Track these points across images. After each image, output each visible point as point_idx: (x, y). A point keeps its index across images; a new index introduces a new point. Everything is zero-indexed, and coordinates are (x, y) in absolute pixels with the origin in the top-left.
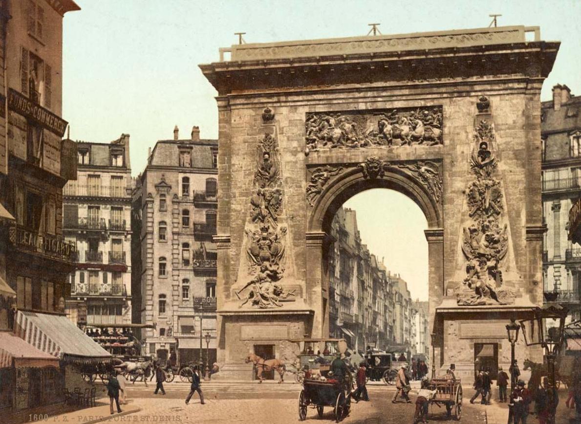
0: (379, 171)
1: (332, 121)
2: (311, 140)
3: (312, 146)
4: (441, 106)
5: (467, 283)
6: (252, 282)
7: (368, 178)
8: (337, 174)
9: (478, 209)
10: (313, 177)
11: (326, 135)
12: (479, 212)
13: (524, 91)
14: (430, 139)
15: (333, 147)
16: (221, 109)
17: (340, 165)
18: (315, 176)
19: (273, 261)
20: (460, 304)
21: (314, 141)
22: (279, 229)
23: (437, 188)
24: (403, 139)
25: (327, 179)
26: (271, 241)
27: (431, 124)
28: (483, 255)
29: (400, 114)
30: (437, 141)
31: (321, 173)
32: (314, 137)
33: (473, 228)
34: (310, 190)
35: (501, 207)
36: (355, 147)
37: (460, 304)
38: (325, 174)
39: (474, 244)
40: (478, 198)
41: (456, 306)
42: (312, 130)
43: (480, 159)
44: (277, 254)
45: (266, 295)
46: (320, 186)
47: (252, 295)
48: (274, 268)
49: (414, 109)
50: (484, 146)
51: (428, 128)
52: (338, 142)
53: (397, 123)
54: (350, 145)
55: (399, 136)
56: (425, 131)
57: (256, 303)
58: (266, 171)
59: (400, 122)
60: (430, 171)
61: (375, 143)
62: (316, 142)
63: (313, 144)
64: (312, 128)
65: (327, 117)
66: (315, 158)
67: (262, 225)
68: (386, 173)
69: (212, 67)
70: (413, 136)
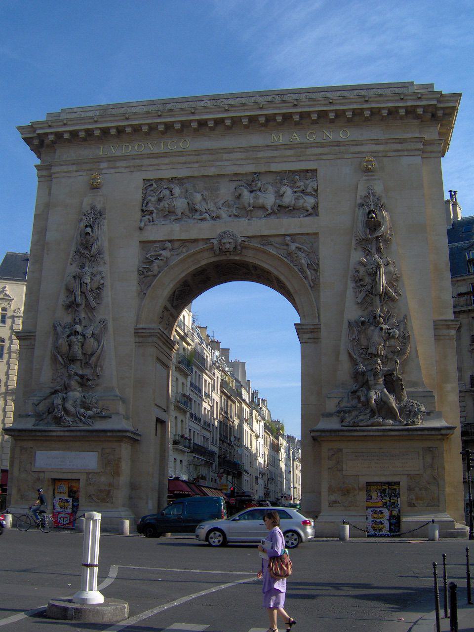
0: (235, 248)
4: (315, 171)
10: (148, 256)
13: (420, 153)
16: (43, 179)
17: (184, 242)
20: (343, 424)
21: (152, 213)
27: (303, 191)
31: (158, 253)
35: (397, 293)
36: (202, 220)
37: (343, 424)
38: (164, 253)
39: (364, 342)
40: (367, 280)
42: (150, 200)
46: (156, 268)
51: (299, 196)
53: (260, 190)
55: (263, 207)
56: (297, 199)
57: (58, 420)
61: (230, 216)
62: (154, 215)
64: (150, 198)
69: (32, 127)
70: (279, 206)
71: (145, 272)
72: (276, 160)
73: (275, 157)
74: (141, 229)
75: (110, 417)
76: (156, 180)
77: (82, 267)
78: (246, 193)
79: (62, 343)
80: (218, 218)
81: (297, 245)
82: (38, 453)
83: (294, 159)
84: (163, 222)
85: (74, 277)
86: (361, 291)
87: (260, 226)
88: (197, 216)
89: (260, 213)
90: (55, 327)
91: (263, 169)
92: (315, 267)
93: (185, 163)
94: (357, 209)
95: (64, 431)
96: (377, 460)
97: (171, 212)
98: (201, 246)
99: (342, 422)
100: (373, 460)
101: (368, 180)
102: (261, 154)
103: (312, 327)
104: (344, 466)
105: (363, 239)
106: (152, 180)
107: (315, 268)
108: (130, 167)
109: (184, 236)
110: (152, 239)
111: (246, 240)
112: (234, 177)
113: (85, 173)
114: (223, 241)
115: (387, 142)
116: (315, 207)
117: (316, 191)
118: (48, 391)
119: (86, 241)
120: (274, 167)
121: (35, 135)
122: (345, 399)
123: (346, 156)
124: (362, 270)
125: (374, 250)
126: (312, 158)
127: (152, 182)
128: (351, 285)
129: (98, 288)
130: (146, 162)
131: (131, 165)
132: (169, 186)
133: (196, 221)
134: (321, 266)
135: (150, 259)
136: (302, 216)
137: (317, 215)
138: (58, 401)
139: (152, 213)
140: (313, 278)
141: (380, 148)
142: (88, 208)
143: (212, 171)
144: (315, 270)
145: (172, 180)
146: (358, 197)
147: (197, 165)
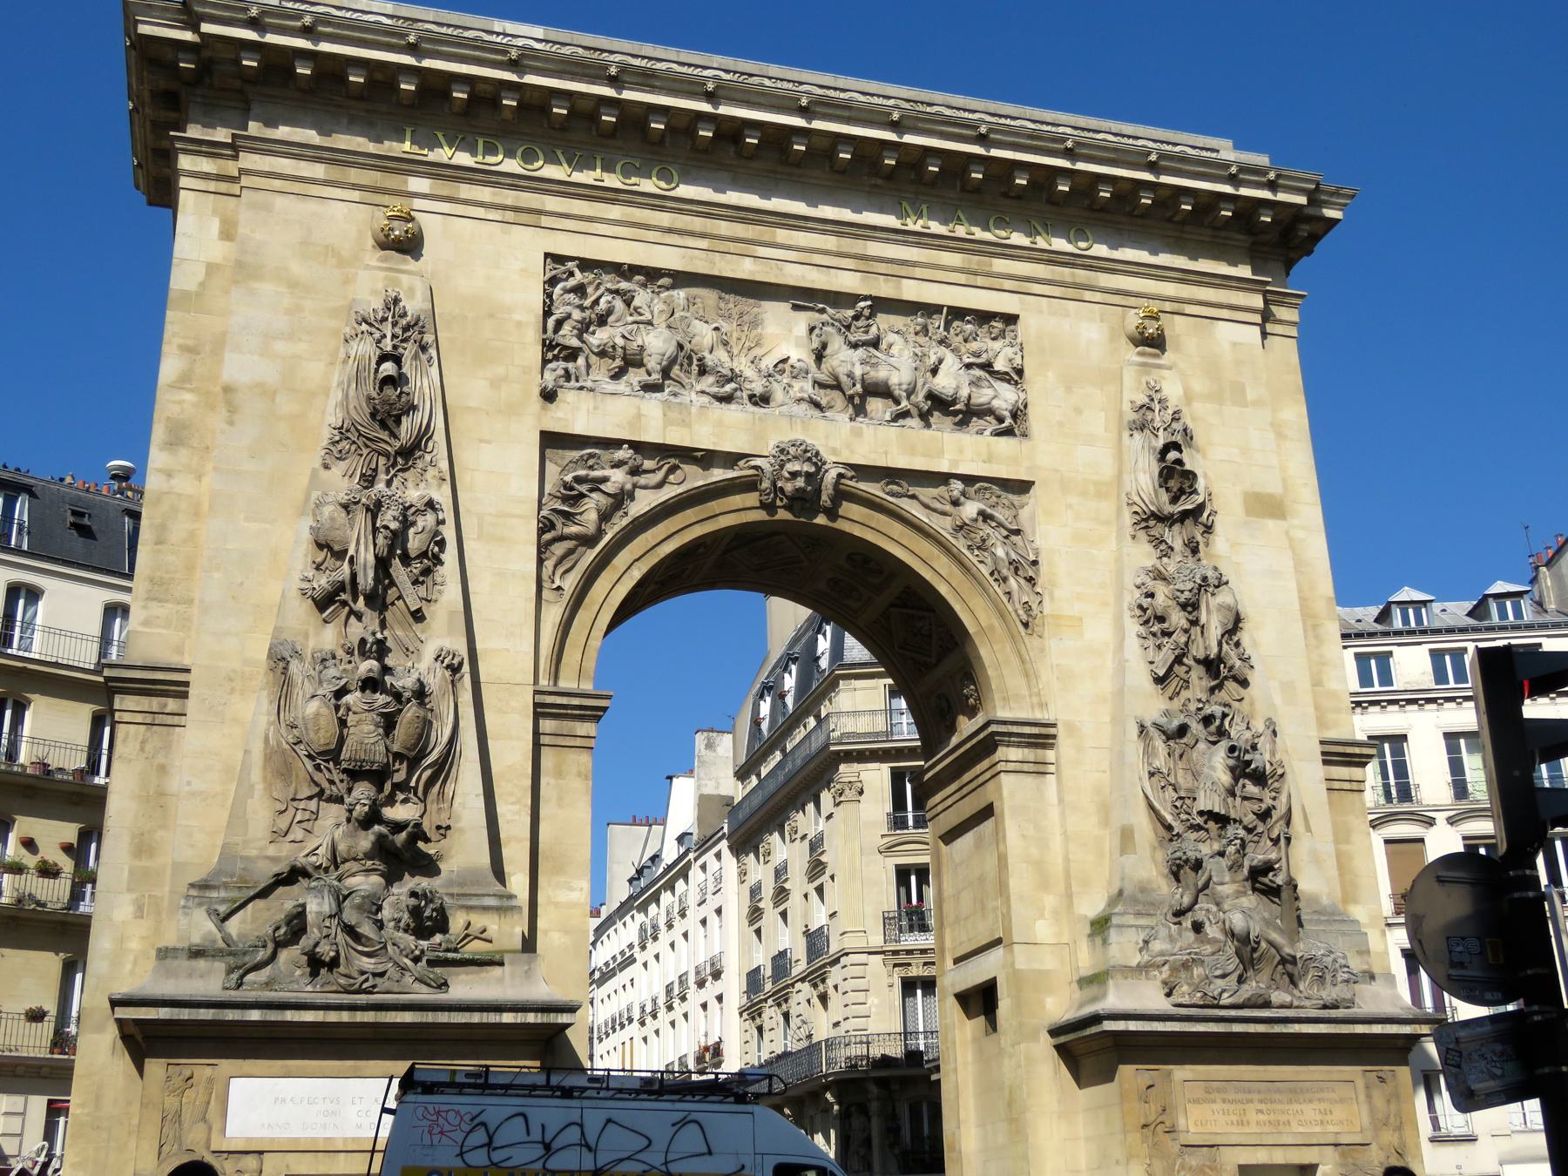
1: (642, 298)
2: (565, 347)
3: (566, 370)
4: (1011, 319)
5: (1187, 922)
6: (294, 875)
7: (783, 515)
8: (660, 485)
9: (1178, 660)
10: (568, 478)
11: (620, 342)
12: (1177, 669)
14: (986, 412)
15: (649, 388)
18: (578, 480)
19: (402, 787)
20: (1176, 999)
21: (573, 355)
22: (429, 651)
23: (1022, 582)
24: (897, 402)
25: (621, 499)
26: (397, 696)
28: (1222, 820)
29: (884, 321)
30: (1008, 421)
32: (575, 342)
33: (1176, 723)
34: (552, 526)
35: (1245, 660)
36: (727, 399)
37: (1176, 999)
38: (618, 477)
40: (1178, 619)
41: (1160, 1004)
42: (569, 316)
43: (1165, 497)
44: (423, 754)
45: (366, 929)
46: (592, 516)
47: (296, 925)
48: (399, 812)
49: (930, 310)
50: (1173, 455)
51: (979, 379)
52: (666, 372)
54: (715, 390)
55: (882, 391)
58: (383, 425)
59: (883, 346)
60: (992, 518)
62: (581, 361)
63: (570, 365)
64: (568, 309)
65: (624, 285)
66: (580, 414)
67: (356, 630)
68: (848, 508)
70: (931, 396)
71: (559, 526)
72: (918, 272)
73: (914, 264)
74: (549, 396)
75: (501, 964)
76: (586, 264)
77: (369, 480)
78: (836, 344)
79: (317, 715)
80: (762, 400)
81: (983, 507)
82: (236, 1085)
83: (962, 278)
84: (611, 386)
85: (345, 507)
86: (1159, 647)
87: (878, 441)
88: (708, 382)
89: (875, 405)
90: (280, 661)
91: (885, 289)
92: (1026, 569)
93: (670, 231)
94: (1126, 434)
95: (353, 1008)
96: (1261, 1101)
97: (632, 361)
98: (718, 474)
99: (1168, 995)
100: (1251, 1101)
101: (1144, 365)
102: (875, 248)
103: (1035, 730)
104: (1182, 1122)
105: (1153, 514)
106: (572, 259)
107: (1031, 573)
108: (504, 208)
109: (676, 437)
110: (579, 427)
111: (850, 474)
112: (802, 297)
113: (356, 195)
114: (794, 466)
115: (1186, 277)
116: (1018, 413)
117: (1020, 372)
118: (265, 872)
119: (384, 402)
120: (911, 291)
121: (188, 36)
122: (1163, 932)
123: (1088, 295)
124: (1162, 591)
125: (1178, 545)
126: (1008, 284)
127: (570, 264)
128: (1133, 627)
129: (424, 555)
130: (552, 203)
131: (509, 202)
132: (624, 285)
133: (705, 399)
134: (1044, 567)
135: (572, 489)
136: (987, 433)
137: (1025, 435)
138: (317, 906)
139: (573, 355)
140: (1025, 599)
141: (1170, 289)
142: (378, 304)
143: (745, 269)
144: (1030, 580)
145: (626, 271)
146: (1127, 407)
147: (703, 243)
